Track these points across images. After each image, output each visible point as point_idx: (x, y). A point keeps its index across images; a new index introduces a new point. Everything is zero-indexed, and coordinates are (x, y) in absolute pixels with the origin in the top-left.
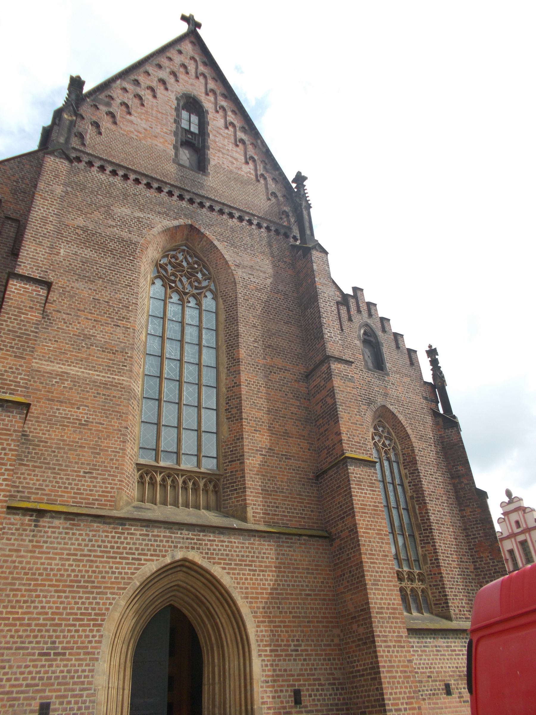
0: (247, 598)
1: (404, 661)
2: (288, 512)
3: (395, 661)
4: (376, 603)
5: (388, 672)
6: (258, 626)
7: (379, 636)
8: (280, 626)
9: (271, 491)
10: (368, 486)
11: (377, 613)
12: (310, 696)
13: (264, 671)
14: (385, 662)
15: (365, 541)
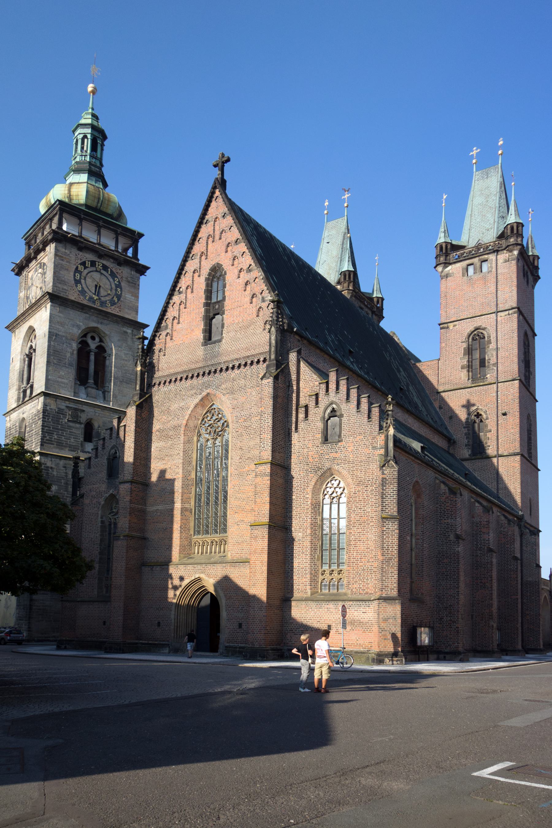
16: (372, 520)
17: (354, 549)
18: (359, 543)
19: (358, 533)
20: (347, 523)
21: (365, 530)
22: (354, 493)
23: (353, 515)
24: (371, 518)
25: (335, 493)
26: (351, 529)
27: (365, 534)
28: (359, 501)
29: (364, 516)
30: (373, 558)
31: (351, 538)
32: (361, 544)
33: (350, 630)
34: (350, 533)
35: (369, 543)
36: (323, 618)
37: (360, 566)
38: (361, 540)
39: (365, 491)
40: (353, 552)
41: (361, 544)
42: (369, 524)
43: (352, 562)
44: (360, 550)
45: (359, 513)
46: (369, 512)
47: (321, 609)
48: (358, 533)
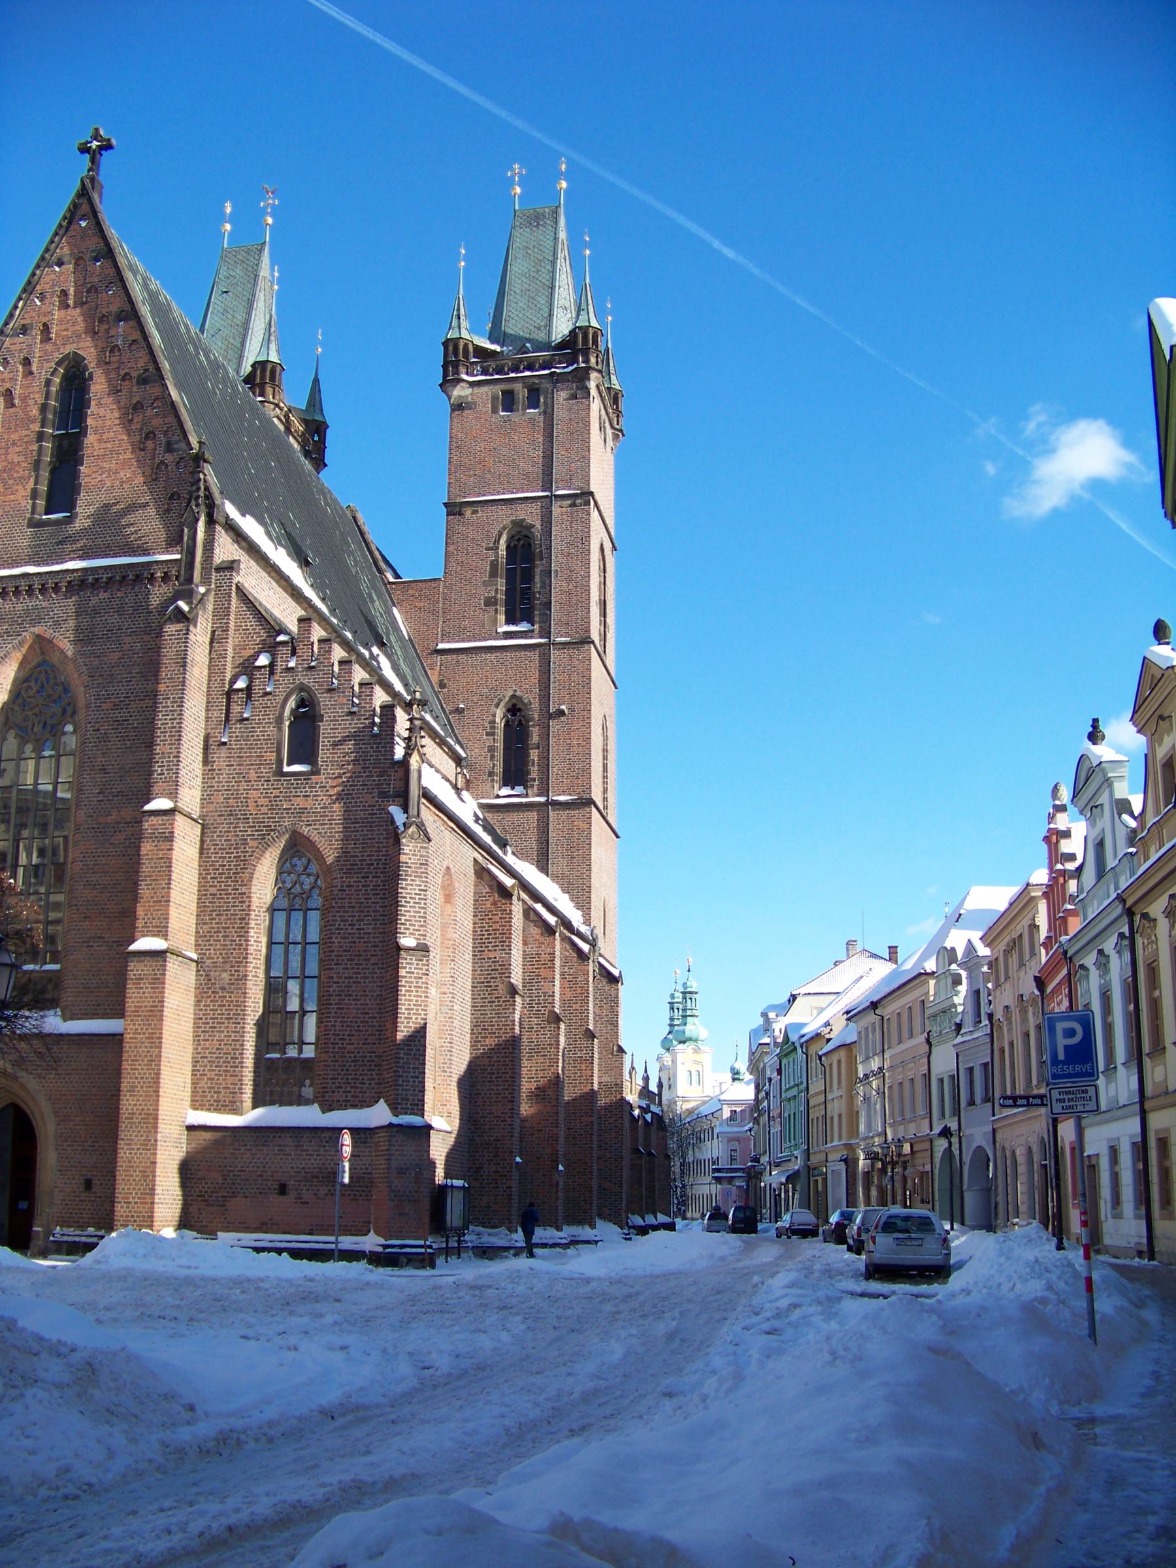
0: (50, 1099)
1: (146, 1163)
2: (111, 1009)
3: (135, 1162)
4: (127, 1109)
5: (124, 1171)
6: (59, 1124)
7: (123, 1140)
8: (79, 1125)
9: (95, 987)
10: (149, 983)
11: (126, 1118)
12: (101, 1184)
13: (59, 1162)
14: (124, 1162)
15: (130, 1047)
16: (375, 951)
17: (336, 1013)
18: (346, 1001)
19: (346, 978)
20: (322, 956)
21: (359, 973)
22: (340, 890)
23: (336, 938)
24: (373, 946)
25: (297, 886)
26: (332, 969)
27: (360, 982)
28: (349, 907)
29: (359, 942)
30: (375, 1035)
31: (331, 989)
32: (351, 1004)
33: (326, 1194)
34: (329, 978)
35: (368, 1002)
36: (270, 1167)
37: (349, 1052)
38: (351, 995)
39: (363, 886)
40: (335, 1022)
41: (351, 1004)
42: (369, 960)
43: (333, 1044)
44: (348, 1018)
45: (349, 934)
46: (370, 933)
47: (265, 1148)
48: (346, 978)
